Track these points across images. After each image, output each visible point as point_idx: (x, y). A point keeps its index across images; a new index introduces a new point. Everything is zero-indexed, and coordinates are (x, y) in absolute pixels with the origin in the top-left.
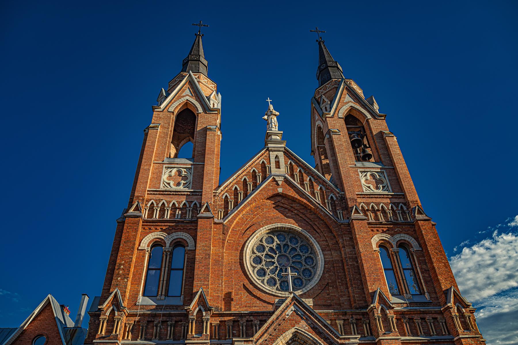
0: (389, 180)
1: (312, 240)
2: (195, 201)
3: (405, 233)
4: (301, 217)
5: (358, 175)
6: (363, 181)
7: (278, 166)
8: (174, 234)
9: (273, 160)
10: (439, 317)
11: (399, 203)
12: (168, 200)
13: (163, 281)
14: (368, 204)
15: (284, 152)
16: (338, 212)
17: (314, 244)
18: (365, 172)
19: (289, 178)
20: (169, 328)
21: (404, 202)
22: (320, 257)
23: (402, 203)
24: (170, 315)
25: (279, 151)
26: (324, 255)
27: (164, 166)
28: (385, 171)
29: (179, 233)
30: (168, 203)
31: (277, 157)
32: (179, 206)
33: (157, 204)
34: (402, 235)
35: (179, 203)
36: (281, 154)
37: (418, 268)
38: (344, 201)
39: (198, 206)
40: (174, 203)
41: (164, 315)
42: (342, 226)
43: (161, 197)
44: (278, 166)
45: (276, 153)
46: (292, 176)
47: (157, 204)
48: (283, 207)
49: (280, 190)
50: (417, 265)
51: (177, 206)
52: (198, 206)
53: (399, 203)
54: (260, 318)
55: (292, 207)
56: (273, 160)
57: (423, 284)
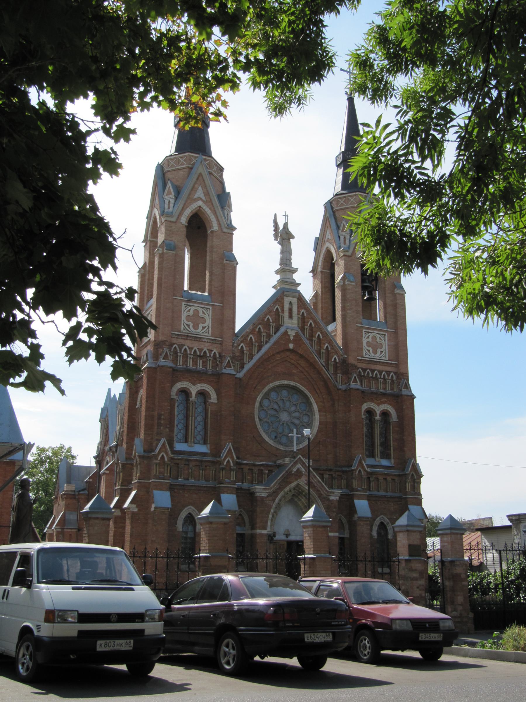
0: (388, 345)
1: (312, 400)
2: (215, 350)
3: (388, 404)
4: (305, 375)
5: (362, 336)
6: (365, 341)
7: (291, 317)
8: (199, 385)
9: (286, 307)
10: (397, 479)
11: (390, 372)
12: (191, 346)
13: (191, 429)
14: (364, 370)
15: (298, 299)
16: (338, 375)
17: (313, 404)
18: (369, 332)
19: (300, 332)
20: (201, 472)
21: (395, 371)
22: (317, 416)
23: (394, 373)
24: (201, 461)
25: (294, 297)
26: (320, 415)
27: (183, 303)
28: (386, 334)
29: (203, 385)
30: (191, 349)
31: (291, 303)
32: (200, 354)
33: (181, 350)
34: (387, 405)
35: (201, 350)
36: (295, 301)
37: (391, 437)
38: (345, 364)
39: (218, 356)
40: (195, 350)
41: (197, 460)
42: (340, 391)
43: (182, 342)
44: (291, 317)
45: (291, 299)
46: (302, 329)
47: (181, 350)
48: (290, 362)
49: (291, 346)
50: (391, 434)
51: (198, 354)
52: (218, 356)
53: (390, 372)
54: (269, 468)
55: (298, 363)
56: (286, 307)
57: (392, 450)
